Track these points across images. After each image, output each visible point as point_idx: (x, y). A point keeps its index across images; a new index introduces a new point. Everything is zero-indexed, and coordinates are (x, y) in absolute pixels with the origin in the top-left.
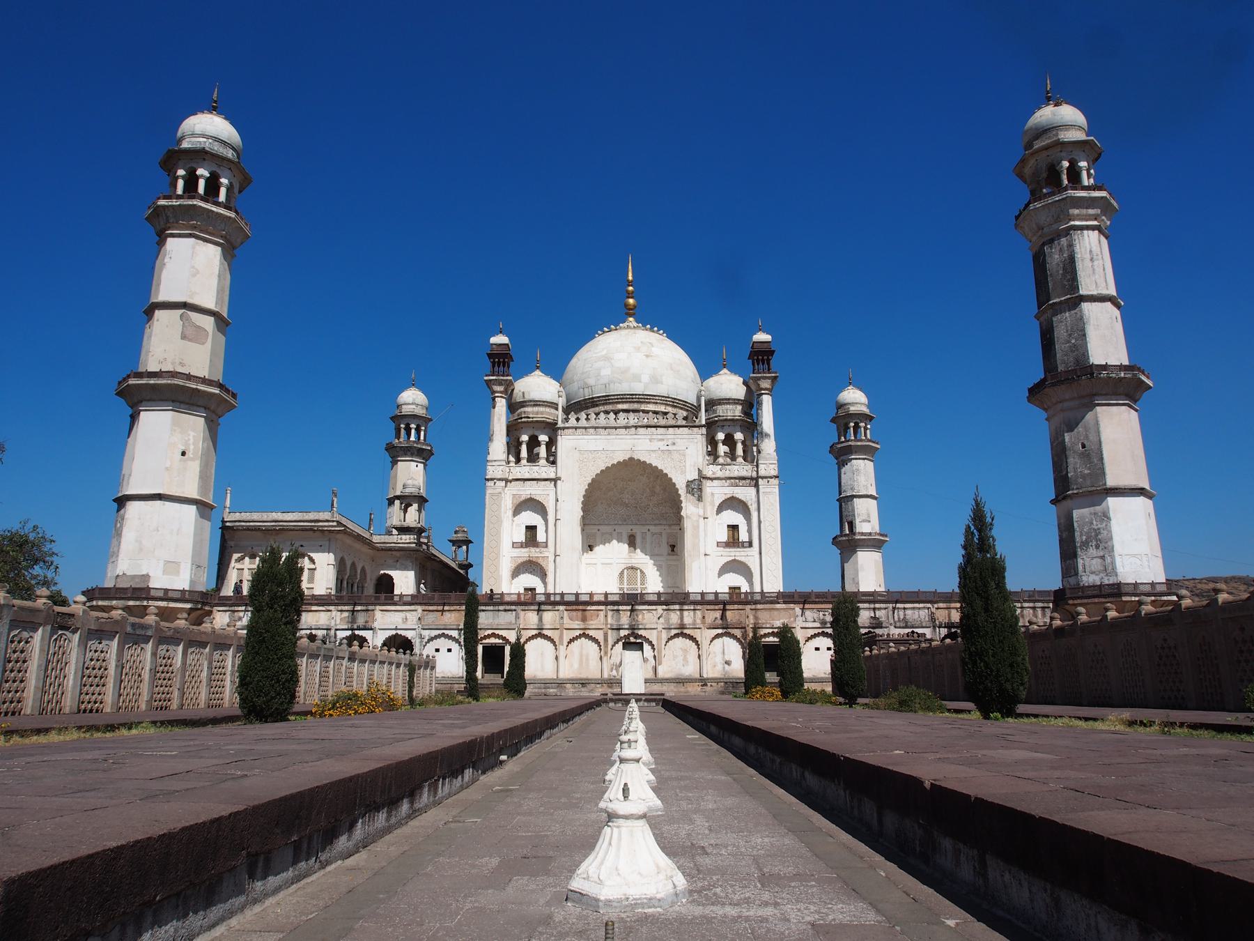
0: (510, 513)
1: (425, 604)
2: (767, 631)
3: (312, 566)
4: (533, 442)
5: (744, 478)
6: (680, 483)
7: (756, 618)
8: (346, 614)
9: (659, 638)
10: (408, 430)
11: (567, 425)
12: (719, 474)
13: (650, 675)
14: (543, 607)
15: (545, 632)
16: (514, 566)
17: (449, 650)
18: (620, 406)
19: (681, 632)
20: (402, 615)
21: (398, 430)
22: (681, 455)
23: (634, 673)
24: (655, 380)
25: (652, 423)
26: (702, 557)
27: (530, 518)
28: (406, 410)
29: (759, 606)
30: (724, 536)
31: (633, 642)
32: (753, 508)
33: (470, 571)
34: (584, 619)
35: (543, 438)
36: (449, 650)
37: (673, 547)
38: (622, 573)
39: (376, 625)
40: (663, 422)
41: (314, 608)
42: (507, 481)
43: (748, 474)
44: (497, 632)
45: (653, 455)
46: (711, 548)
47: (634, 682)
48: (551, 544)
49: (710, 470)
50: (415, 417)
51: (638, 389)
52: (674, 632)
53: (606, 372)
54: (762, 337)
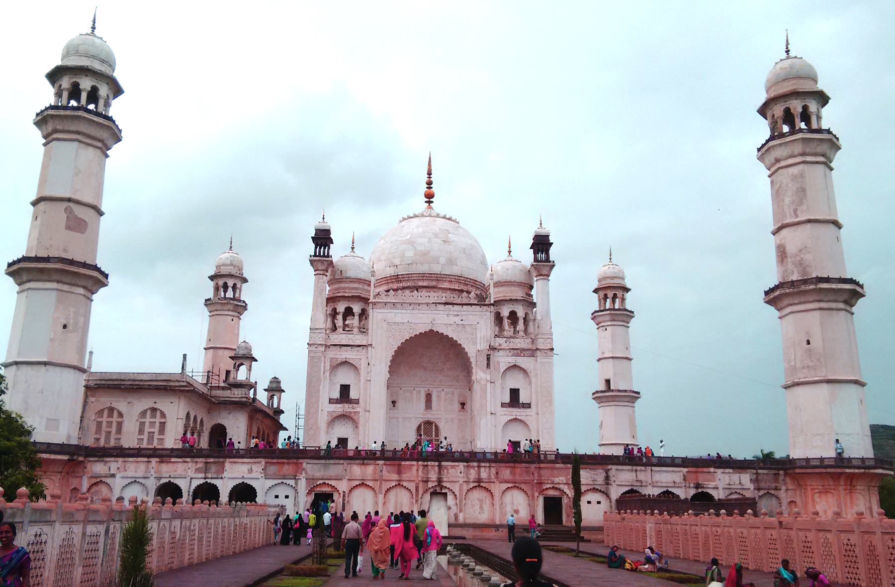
0: (328, 374)
1: (268, 458)
2: (548, 486)
3: (163, 420)
4: (349, 312)
5: (524, 350)
6: (471, 350)
7: (540, 475)
8: (199, 465)
9: (461, 490)
10: (225, 287)
11: (377, 300)
12: (504, 346)
13: (452, 520)
14: (366, 461)
15: (368, 483)
16: (330, 419)
17: (287, 497)
18: (420, 284)
19: (479, 484)
20: (249, 466)
21: (217, 289)
22: (473, 330)
23: (440, 517)
24: (451, 262)
25: (450, 301)
26: (489, 416)
27: (344, 377)
28: (224, 270)
29: (542, 465)
30: (507, 399)
31: (439, 493)
32: (532, 375)
33: (282, 416)
34: (399, 473)
35: (357, 308)
36: (287, 497)
37: (463, 404)
38: (420, 426)
39: (225, 474)
40: (459, 302)
41: (173, 460)
42: (326, 346)
43: (530, 346)
44: (327, 482)
45: (450, 328)
48: (361, 401)
50: (231, 276)
51: (436, 269)
52: (472, 485)
53: (410, 254)
54: (542, 232)
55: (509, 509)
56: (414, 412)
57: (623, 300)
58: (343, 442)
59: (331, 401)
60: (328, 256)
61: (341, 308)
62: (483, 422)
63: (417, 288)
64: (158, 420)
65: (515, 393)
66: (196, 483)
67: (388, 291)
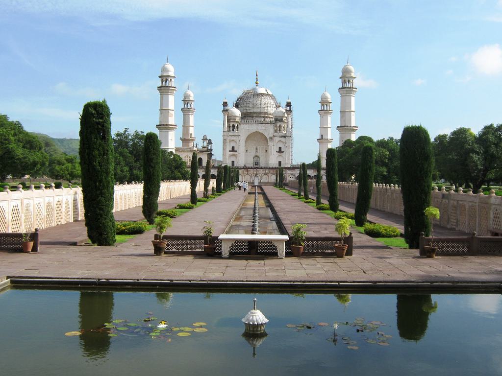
5: (282, 136)
6: (268, 137)
19: (266, 174)
22: (269, 131)
37: (266, 151)
43: (284, 135)
46: (274, 152)
47: (256, 183)
49: (275, 134)
54: (289, 101)
55: (272, 179)
56: (253, 153)
57: (329, 106)
58: (233, 162)
59: (230, 151)
60: (227, 110)
61: (231, 125)
62: (271, 157)
63: (253, 117)
64: (189, 158)
65: (280, 148)
66: (202, 174)
67: (245, 117)
